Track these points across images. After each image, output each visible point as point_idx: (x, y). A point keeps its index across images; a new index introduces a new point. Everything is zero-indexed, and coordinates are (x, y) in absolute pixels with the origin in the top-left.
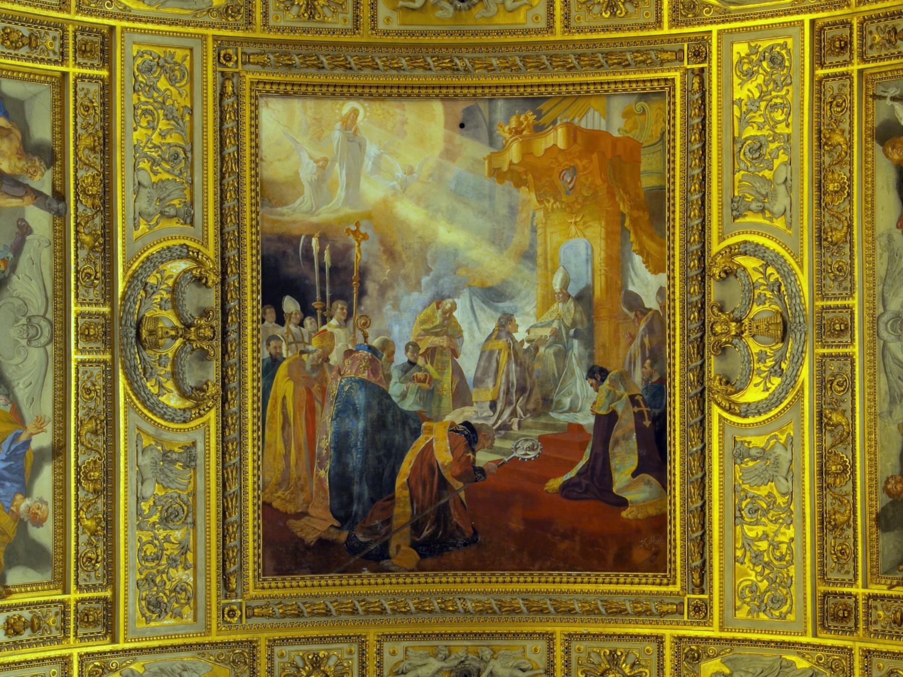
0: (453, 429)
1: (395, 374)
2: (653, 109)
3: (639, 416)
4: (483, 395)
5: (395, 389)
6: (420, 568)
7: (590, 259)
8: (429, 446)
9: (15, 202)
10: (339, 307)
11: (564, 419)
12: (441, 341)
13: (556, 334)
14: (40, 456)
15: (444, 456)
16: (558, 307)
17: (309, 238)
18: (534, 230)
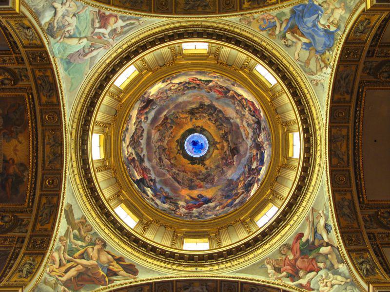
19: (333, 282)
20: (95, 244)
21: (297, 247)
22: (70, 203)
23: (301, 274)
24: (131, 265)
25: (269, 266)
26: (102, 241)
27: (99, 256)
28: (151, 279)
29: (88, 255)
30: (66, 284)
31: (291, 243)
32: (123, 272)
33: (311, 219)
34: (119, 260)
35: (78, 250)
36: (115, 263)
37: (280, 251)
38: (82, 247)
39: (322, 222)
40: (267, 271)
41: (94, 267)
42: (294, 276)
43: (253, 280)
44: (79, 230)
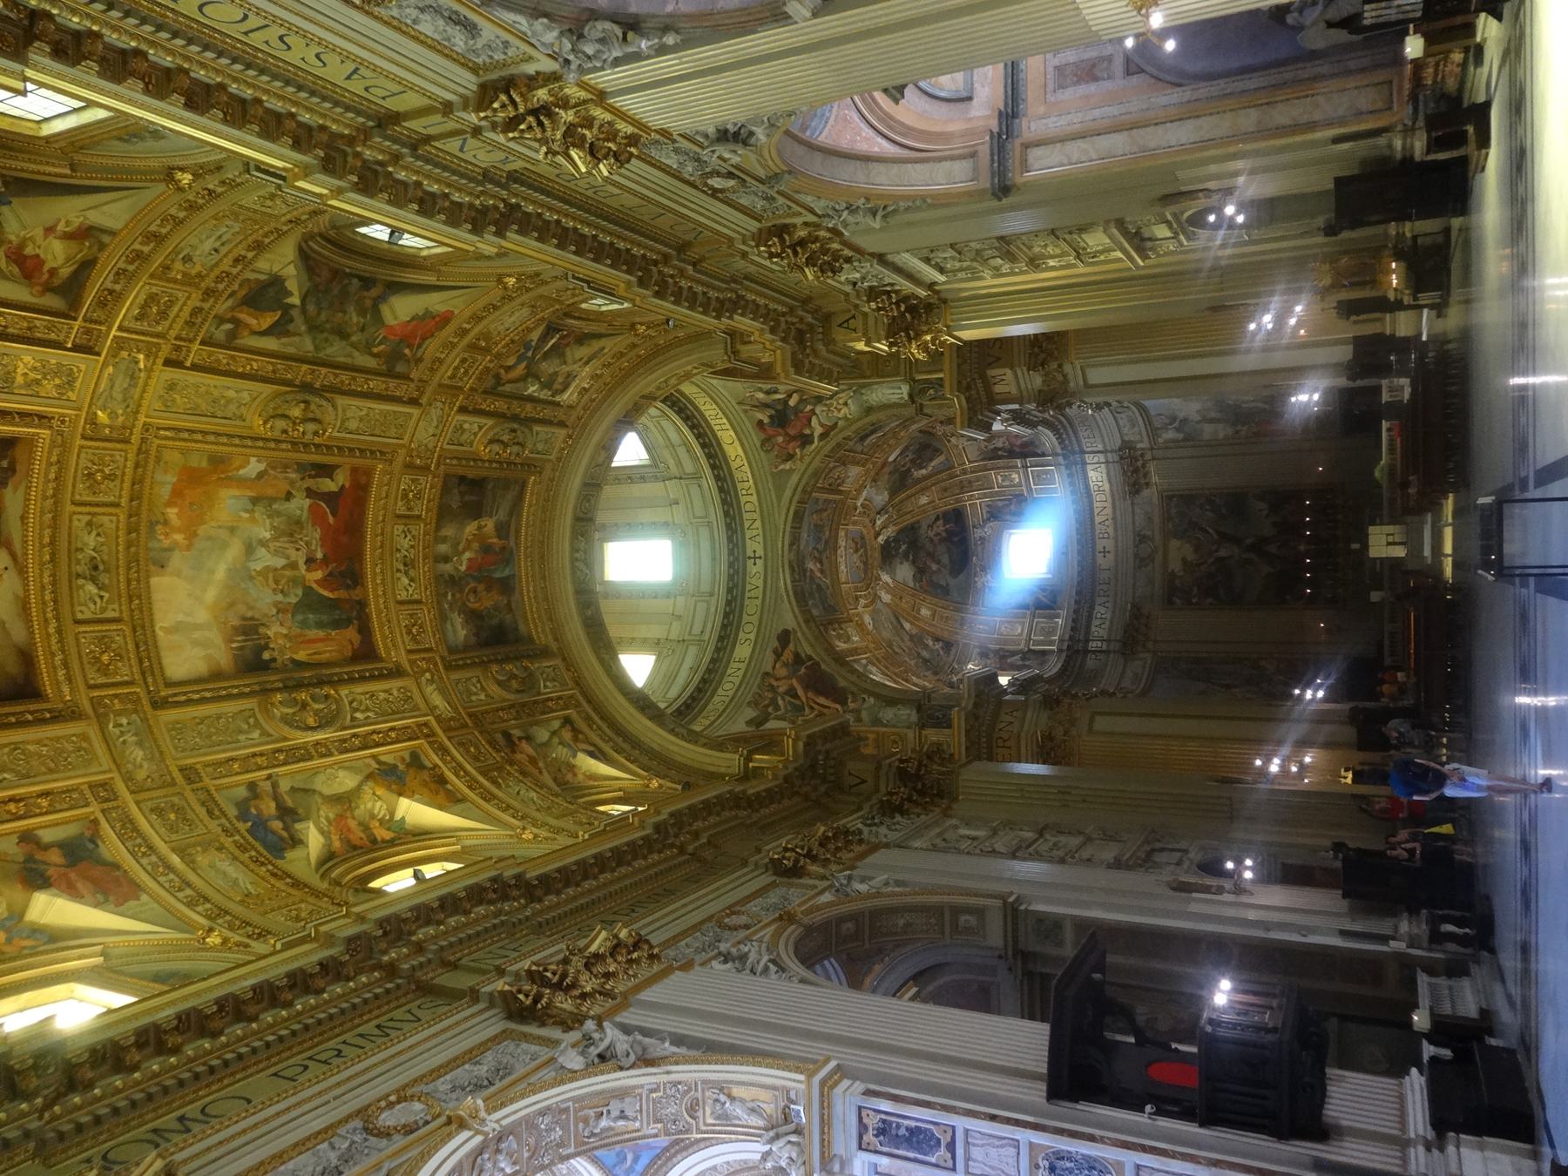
0: (308, 570)
1: (288, 600)
2: (168, 455)
3: (310, 477)
4: (293, 554)
5: (294, 600)
6: (363, 585)
7: (237, 497)
8: (316, 582)
9: (286, 797)
10: (262, 630)
11: (305, 514)
12: (271, 575)
13: (269, 517)
14: (379, 762)
15: (319, 575)
16: (257, 515)
17: (232, 649)
18: (220, 527)
19: (841, 401)
20: (771, 686)
21: (771, 431)
23: (807, 431)
25: (781, 467)
27: (784, 678)
30: (843, 703)
31: (763, 436)
32: (791, 646)
34: (778, 654)
35: (790, 702)
38: (783, 699)
39: (761, 396)
41: (800, 680)
42: (806, 440)
44: (767, 706)
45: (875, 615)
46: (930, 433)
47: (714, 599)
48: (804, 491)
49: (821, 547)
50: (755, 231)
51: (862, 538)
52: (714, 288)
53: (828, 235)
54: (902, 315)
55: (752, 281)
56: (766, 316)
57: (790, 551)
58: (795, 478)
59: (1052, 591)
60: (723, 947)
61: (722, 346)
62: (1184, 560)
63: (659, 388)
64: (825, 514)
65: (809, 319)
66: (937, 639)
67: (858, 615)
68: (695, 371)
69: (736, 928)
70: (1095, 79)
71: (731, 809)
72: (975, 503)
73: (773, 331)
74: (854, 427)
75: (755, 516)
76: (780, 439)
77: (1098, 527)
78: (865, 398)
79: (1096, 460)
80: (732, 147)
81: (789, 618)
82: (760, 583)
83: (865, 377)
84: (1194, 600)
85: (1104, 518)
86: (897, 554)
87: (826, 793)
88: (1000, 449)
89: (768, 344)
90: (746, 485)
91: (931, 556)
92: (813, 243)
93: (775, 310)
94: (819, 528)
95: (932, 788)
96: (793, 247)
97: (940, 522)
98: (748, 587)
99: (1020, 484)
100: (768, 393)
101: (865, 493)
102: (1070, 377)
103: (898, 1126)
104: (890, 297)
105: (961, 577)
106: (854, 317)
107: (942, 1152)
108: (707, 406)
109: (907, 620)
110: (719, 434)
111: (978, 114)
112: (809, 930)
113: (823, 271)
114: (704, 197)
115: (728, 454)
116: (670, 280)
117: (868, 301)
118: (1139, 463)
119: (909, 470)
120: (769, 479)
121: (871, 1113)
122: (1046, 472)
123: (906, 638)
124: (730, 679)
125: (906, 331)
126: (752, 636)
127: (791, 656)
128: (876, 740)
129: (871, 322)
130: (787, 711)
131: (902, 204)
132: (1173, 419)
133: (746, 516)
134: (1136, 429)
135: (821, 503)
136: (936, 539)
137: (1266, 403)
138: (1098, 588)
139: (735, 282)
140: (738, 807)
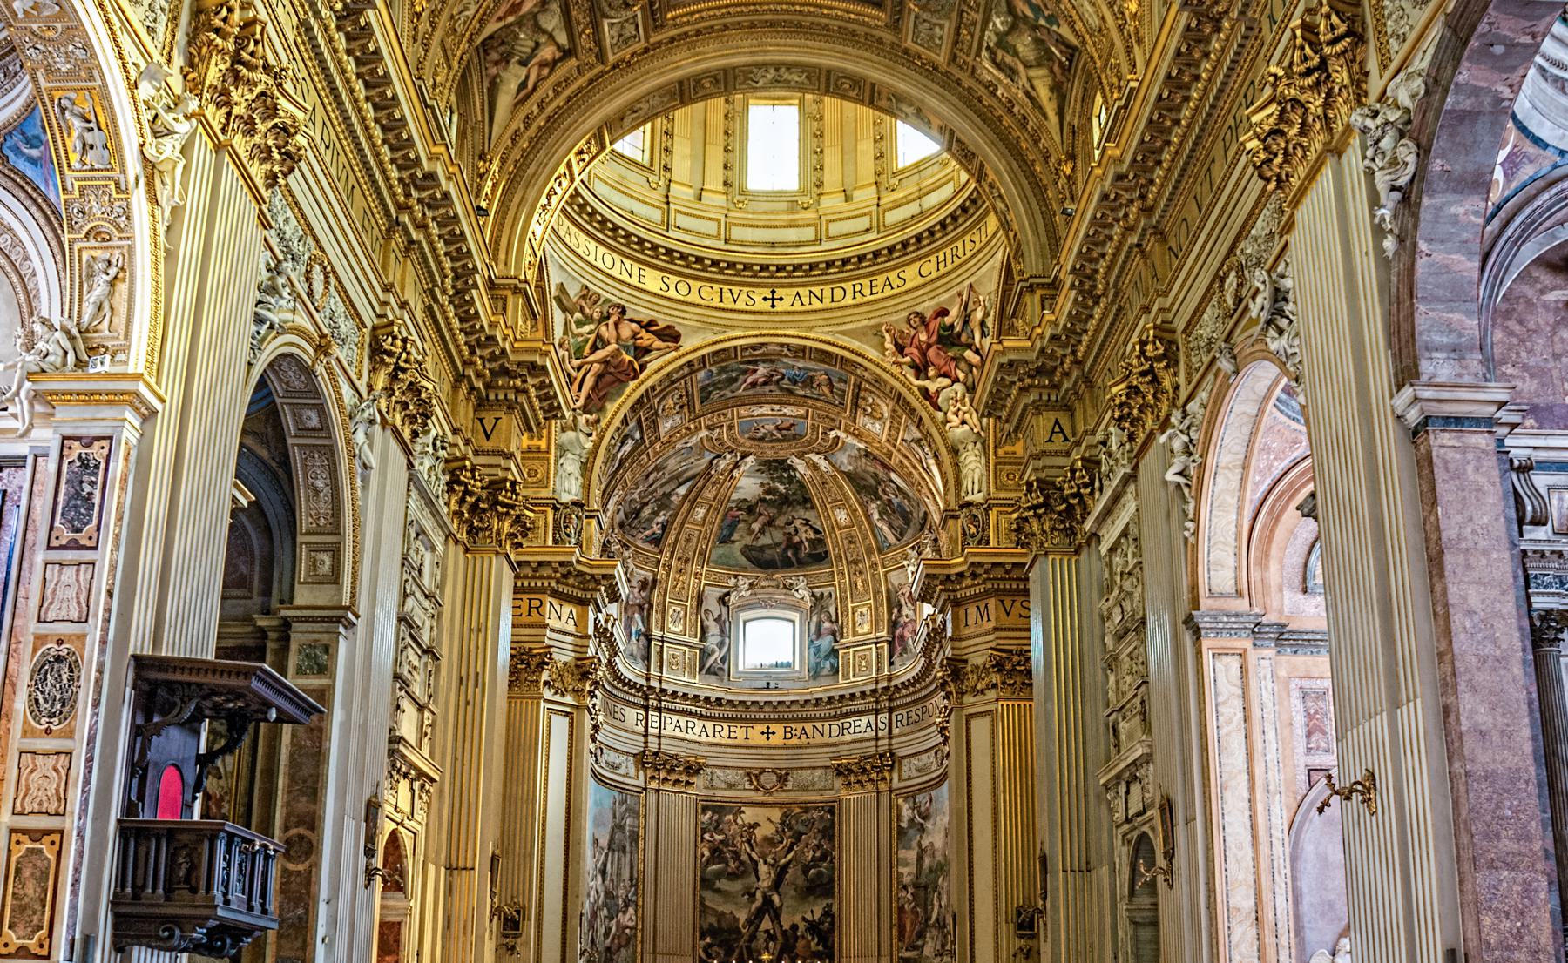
19: (967, 416)
20: (608, 318)
21: (934, 325)
22: (559, 281)
23: (931, 372)
24: (668, 327)
25: (887, 337)
26: (618, 306)
28: (701, 348)
29: (602, 340)
30: (586, 409)
31: (928, 315)
32: (658, 343)
33: (965, 298)
34: (648, 325)
35: (587, 341)
36: (643, 333)
37: (909, 320)
38: (591, 332)
39: (979, 314)
40: (883, 344)
43: (859, 355)
44: (582, 310)
45: (701, 448)
46: (922, 526)
47: (721, 245)
48: (856, 365)
49: (786, 383)
50: (1175, 324)
51: (795, 437)
52: (1110, 268)
53: (1162, 415)
54: (1065, 500)
55: (1116, 315)
56: (1070, 331)
57: (782, 345)
58: (873, 354)
59: (722, 669)
60: (288, 265)
61: (1040, 272)
62: (756, 825)
63: (992, 186)
64: (826, 390)
65: (1067, 385)
66: (664, 527)
67: (698, 429)
68: (1011, 234)
69: (308, 279)
70: (1309, 735)
71: (453, 269)
72: (836, 579)
73: (1054, 338)
74: (934, 432)
75: (827, 300)
76: (923, 337)
77: (800, 726)
78: (970, 447)
79: (880, 725)
80: (1267, 306)
81: (694, 342)
82: (740, 305)
83: (996, 447)
84: (707, 836)
85: (810, 734)
86: (772, 479)
87: (472, 389)
88: (899, 611)
89: (1039, 331)
90: (866, 291)
91: (770, 523)
92: (1154, 395)
93: (1080, 342)
94: (809, 382)
95: (481, 520)
96: (1151, 371)
97: (812, 536)
98: (736, 290)
99: (855, 634)
100: (982, 323)
101: (851, 440)
102: (980, 697)
103: (92, 484)
104: (1085, 486)
105: (743, 561)
106: (1066, 439)
107: (67, 535)
108: (969, 245)
109: (690, 490)
110: (933, 258)
111: (1286, 602)
112: (309, 372)
113: (1121, 405)
114: (1216, 264)
115: (906, 268)
116: (1121, 214)
117: (1083, 459)
118: (874, 776)
119: (879, 498)
120: (873, 322)
121: (105, 451)
122: (868, 667)
123: (667, 489)
124: (618, 263)
125: (1046, 504)
126: (672, 293)
127: (646, 343)
128: (539, 450)
129: (1060, 461)
130: (574, 336)
131: (1192, 505)
132: (925, 817)
133: (827, 289)
134: (915, 773)
135: (842, 386)
136: (791, 529)
137: (937, 920)
138: (725, 725)
139: (1116, 294)
140: (457, 277)
